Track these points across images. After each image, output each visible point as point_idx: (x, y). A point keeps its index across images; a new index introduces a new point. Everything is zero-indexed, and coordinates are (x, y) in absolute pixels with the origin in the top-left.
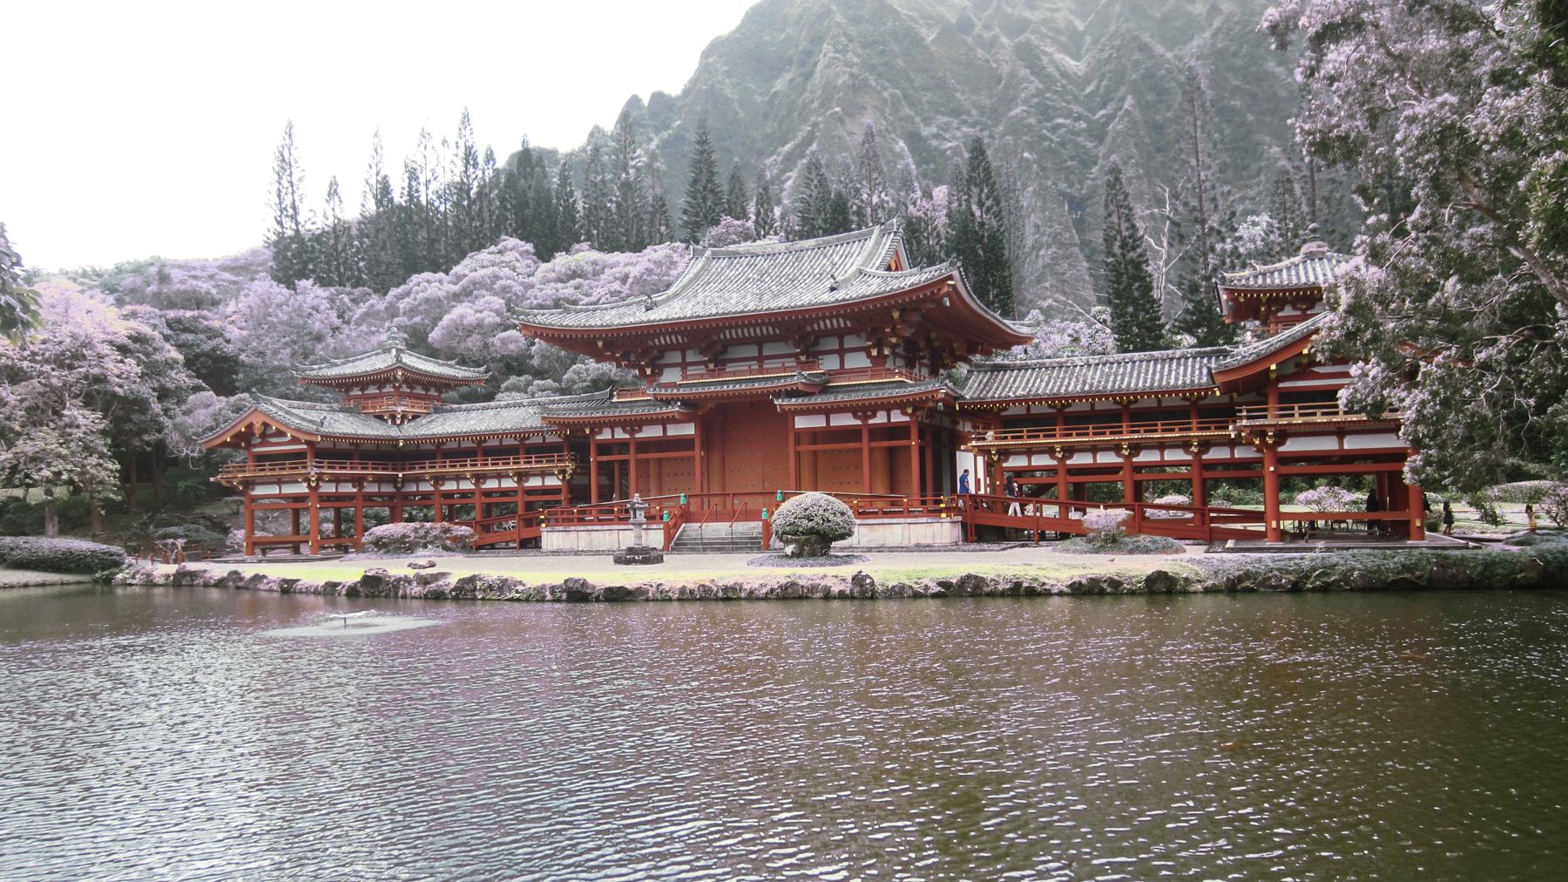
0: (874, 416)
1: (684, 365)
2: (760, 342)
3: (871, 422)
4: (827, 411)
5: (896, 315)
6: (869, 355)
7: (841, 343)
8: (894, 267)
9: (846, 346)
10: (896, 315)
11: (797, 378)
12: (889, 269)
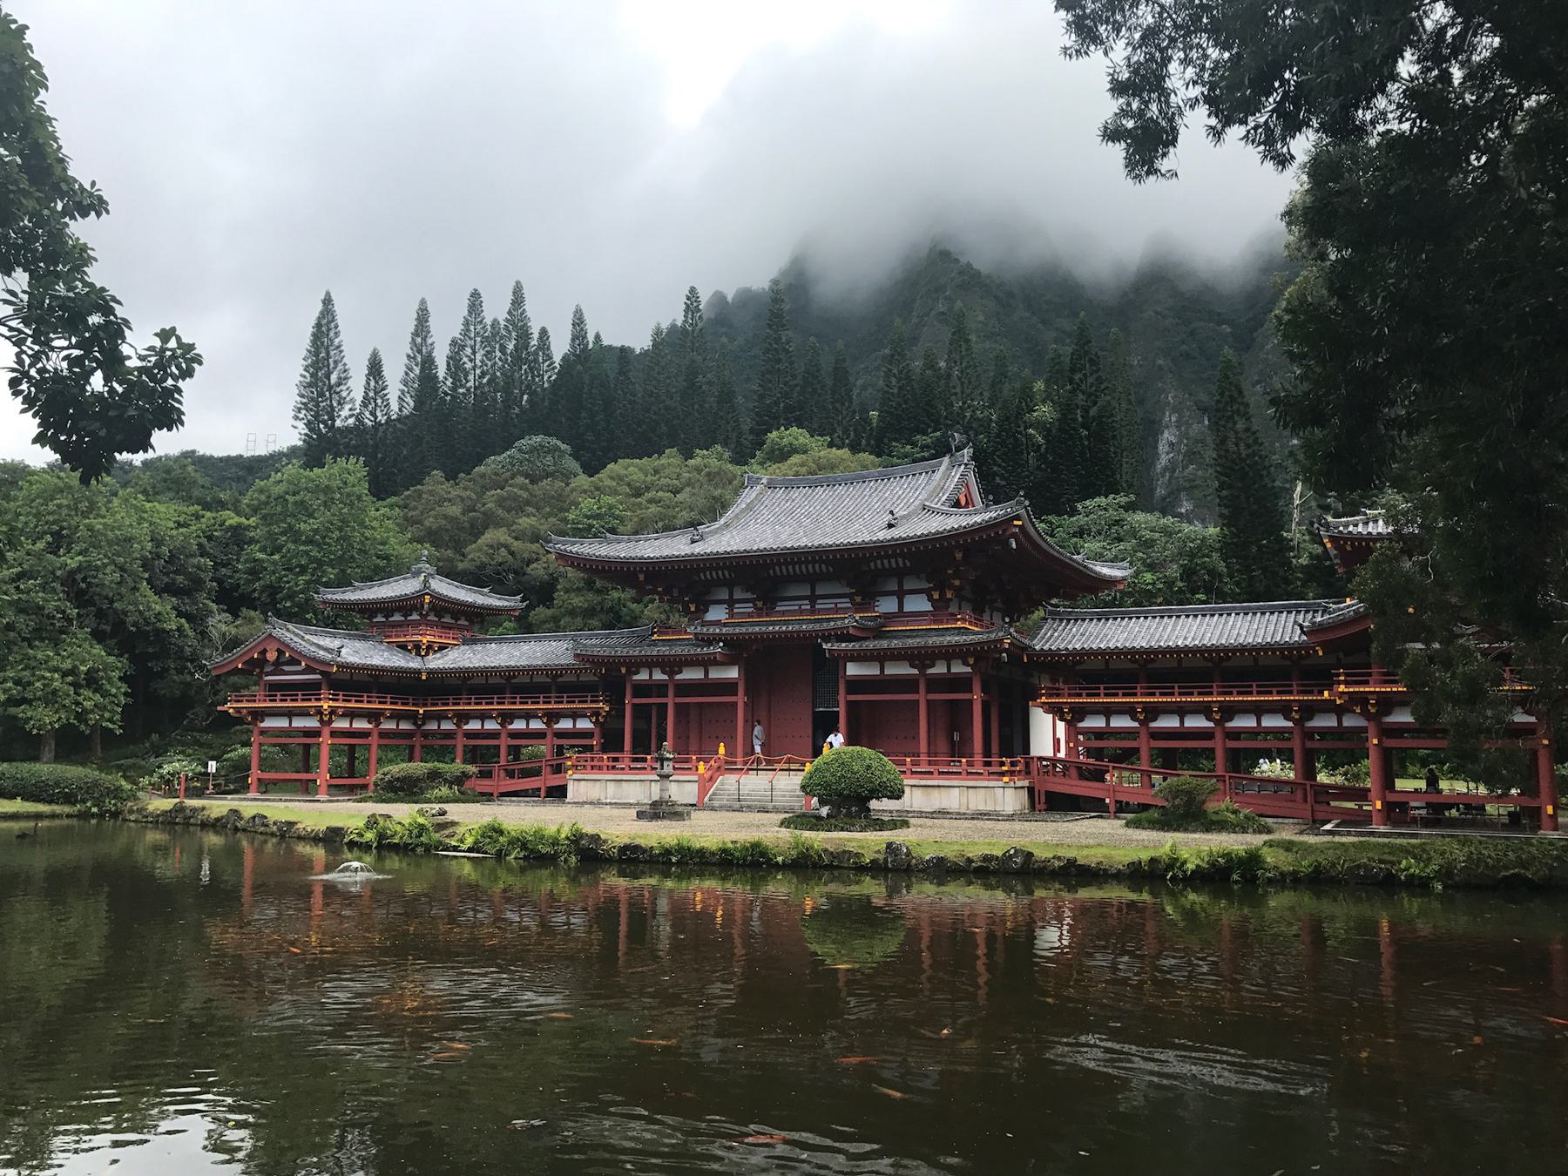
2: (813, 580)
3: (930, 671)
4: (881, 657)
6: (930, 599)
7: (900, 584)
8: (963, 503)
9: (905, 588)
11: (850, 621)
12: (957, 504)
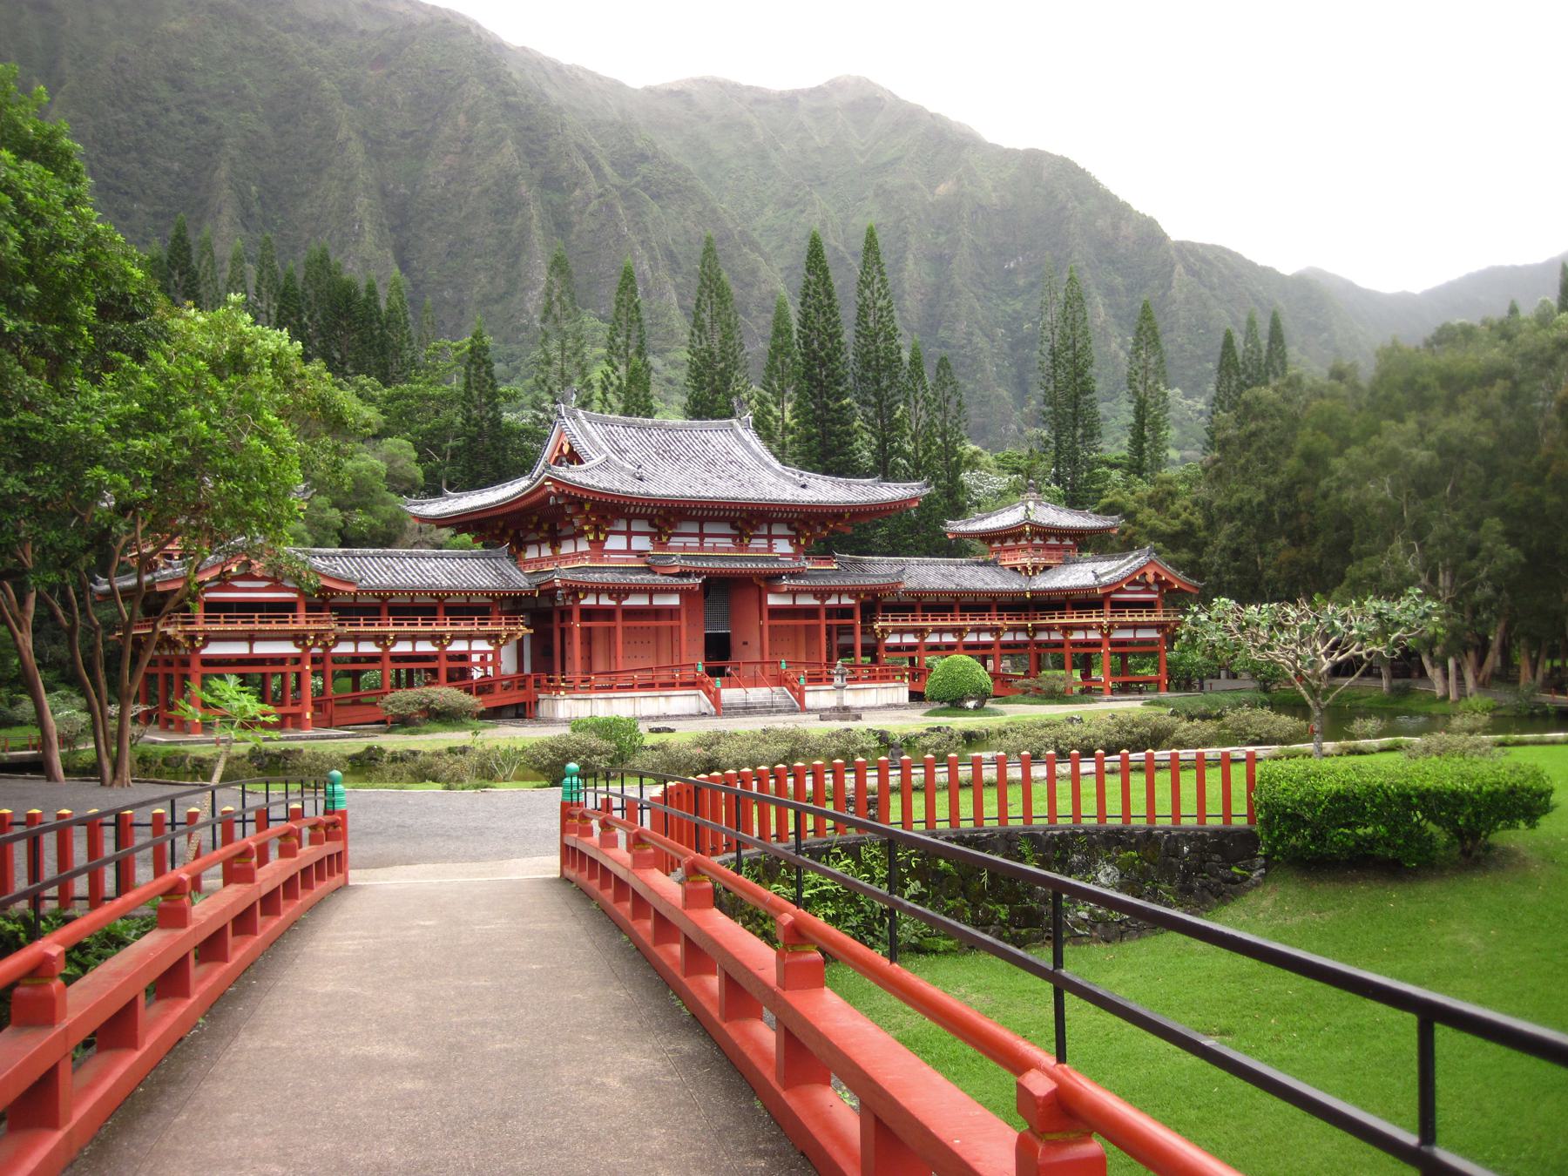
0: (829, 597)
1: (629, 534)
2: (701, 521)
3: (828, 602)
4: (794, 593)
5: (847, 516)
6: (791, 544)
7: (770, 530)
9: (773, 532)
10: (847, 516)
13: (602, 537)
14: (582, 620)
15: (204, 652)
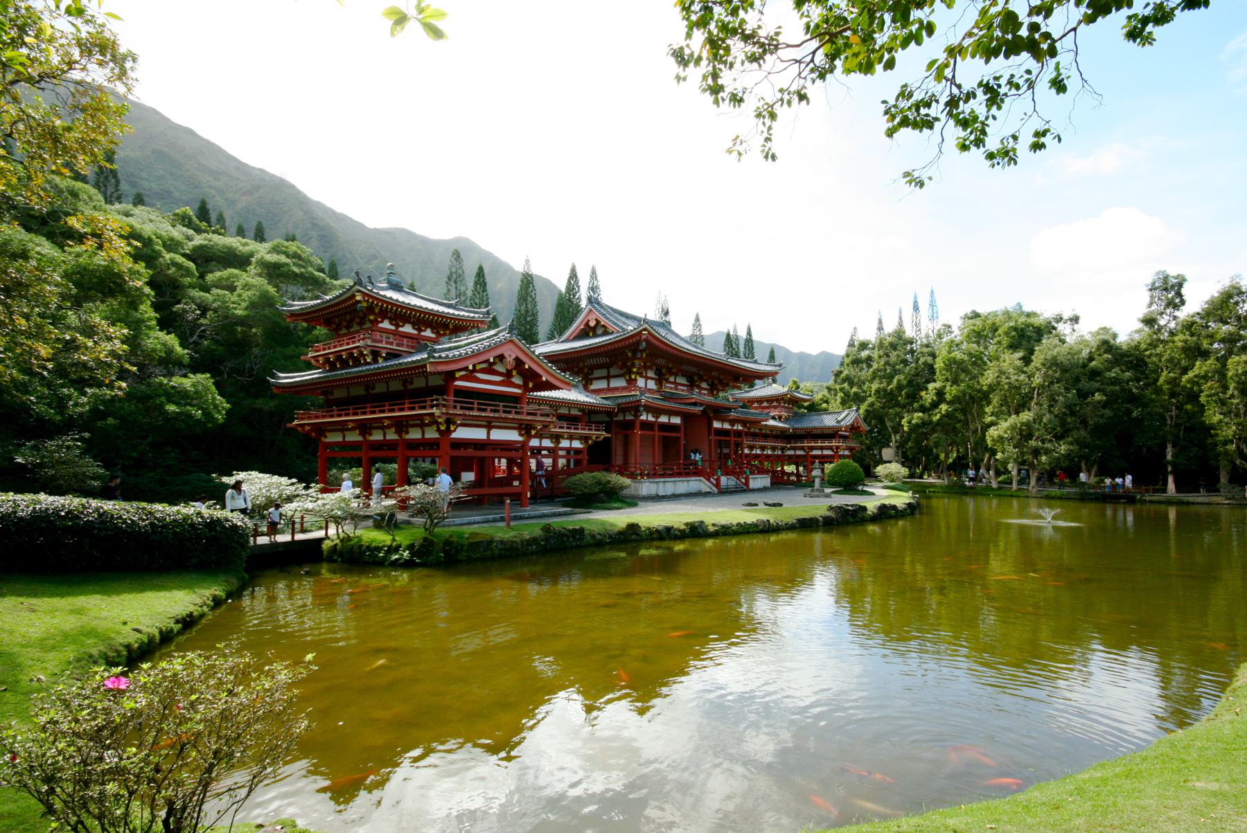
1: (647, 378)
13: (638, 377)
14: (641, 429)
15: (454, 435)
